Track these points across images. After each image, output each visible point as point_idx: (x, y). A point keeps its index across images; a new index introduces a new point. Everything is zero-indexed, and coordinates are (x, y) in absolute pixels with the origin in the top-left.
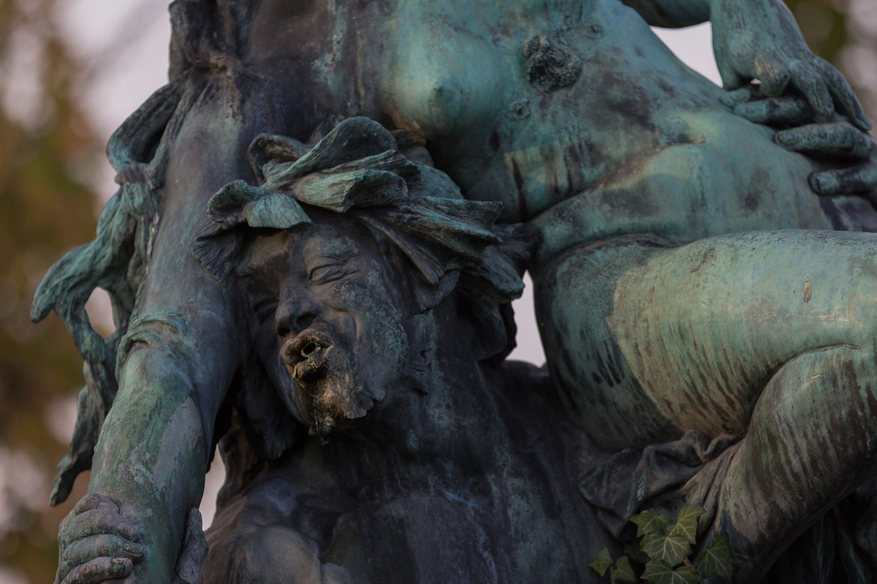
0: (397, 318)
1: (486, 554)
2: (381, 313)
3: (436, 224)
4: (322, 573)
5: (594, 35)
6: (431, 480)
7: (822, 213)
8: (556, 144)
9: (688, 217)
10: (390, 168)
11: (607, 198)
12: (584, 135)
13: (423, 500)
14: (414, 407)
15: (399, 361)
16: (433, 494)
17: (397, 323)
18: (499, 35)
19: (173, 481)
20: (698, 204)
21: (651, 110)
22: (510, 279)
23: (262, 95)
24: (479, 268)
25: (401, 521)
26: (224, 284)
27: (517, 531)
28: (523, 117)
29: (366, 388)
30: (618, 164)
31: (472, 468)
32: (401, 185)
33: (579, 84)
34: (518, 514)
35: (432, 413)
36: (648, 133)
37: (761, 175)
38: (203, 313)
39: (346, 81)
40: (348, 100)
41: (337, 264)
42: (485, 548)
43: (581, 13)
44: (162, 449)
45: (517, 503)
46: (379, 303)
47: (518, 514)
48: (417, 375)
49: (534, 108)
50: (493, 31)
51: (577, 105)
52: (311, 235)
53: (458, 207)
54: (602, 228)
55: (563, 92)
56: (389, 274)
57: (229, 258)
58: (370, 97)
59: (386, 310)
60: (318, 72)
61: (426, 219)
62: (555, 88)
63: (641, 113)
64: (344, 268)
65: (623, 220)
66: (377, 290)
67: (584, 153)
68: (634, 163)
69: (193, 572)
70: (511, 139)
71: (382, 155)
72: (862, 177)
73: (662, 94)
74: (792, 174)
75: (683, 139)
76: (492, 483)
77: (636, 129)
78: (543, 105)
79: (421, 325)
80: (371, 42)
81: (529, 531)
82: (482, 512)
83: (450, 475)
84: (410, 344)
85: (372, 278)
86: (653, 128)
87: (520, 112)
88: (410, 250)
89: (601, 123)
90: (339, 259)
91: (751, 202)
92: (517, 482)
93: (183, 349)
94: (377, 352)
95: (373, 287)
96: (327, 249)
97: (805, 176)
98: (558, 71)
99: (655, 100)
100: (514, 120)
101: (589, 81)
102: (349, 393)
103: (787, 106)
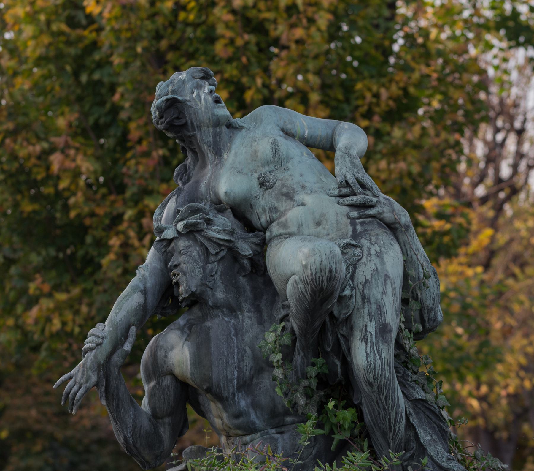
1: (233, 337)
2: (195, 264)
4: (183, 344)
6: (220, 314)
7: (350, 225)
8: (266, 207)
10: (201, 219)
11: (278, 224)
12: (273, 204)
13: (217, 320)
14: (209, 292)
20: (300, 226)
29: (189, 288)
30: (282, 213)
31: (232, 310)
33: (274, 188)
36: (292, 202)
37: (323, 215)
38: (154, 265)
39: (207, 190)
42: (233, 335)
44: (123, 308)
45: (247, 321)
46: (195, 261)
47: (247, 324)
48: (207, 283)
49: (261, 196)
50: (252, 172)
52: (179, 240)
53: (220, 230)
55: (269, 190)
57: (163, 247)
60: (201, 187)
62: (267, 189)
65: (281, 231)
67: (274, 209)
71: (198, 215)
73: (301, 189)
74: (337, 214)
75: (303, 204)
77: (289, 201)
78: (263, 195)
85: (195, 253)
86: (294, 201)
87: (256, 197)
88: (207, 244)
90: (187, 247)
91: (318, 224)
92: (249, 314)
93: (145, 276)
96: (183, 245)
97: (345, 214)
98: (267, 184)
103: (345, 191)
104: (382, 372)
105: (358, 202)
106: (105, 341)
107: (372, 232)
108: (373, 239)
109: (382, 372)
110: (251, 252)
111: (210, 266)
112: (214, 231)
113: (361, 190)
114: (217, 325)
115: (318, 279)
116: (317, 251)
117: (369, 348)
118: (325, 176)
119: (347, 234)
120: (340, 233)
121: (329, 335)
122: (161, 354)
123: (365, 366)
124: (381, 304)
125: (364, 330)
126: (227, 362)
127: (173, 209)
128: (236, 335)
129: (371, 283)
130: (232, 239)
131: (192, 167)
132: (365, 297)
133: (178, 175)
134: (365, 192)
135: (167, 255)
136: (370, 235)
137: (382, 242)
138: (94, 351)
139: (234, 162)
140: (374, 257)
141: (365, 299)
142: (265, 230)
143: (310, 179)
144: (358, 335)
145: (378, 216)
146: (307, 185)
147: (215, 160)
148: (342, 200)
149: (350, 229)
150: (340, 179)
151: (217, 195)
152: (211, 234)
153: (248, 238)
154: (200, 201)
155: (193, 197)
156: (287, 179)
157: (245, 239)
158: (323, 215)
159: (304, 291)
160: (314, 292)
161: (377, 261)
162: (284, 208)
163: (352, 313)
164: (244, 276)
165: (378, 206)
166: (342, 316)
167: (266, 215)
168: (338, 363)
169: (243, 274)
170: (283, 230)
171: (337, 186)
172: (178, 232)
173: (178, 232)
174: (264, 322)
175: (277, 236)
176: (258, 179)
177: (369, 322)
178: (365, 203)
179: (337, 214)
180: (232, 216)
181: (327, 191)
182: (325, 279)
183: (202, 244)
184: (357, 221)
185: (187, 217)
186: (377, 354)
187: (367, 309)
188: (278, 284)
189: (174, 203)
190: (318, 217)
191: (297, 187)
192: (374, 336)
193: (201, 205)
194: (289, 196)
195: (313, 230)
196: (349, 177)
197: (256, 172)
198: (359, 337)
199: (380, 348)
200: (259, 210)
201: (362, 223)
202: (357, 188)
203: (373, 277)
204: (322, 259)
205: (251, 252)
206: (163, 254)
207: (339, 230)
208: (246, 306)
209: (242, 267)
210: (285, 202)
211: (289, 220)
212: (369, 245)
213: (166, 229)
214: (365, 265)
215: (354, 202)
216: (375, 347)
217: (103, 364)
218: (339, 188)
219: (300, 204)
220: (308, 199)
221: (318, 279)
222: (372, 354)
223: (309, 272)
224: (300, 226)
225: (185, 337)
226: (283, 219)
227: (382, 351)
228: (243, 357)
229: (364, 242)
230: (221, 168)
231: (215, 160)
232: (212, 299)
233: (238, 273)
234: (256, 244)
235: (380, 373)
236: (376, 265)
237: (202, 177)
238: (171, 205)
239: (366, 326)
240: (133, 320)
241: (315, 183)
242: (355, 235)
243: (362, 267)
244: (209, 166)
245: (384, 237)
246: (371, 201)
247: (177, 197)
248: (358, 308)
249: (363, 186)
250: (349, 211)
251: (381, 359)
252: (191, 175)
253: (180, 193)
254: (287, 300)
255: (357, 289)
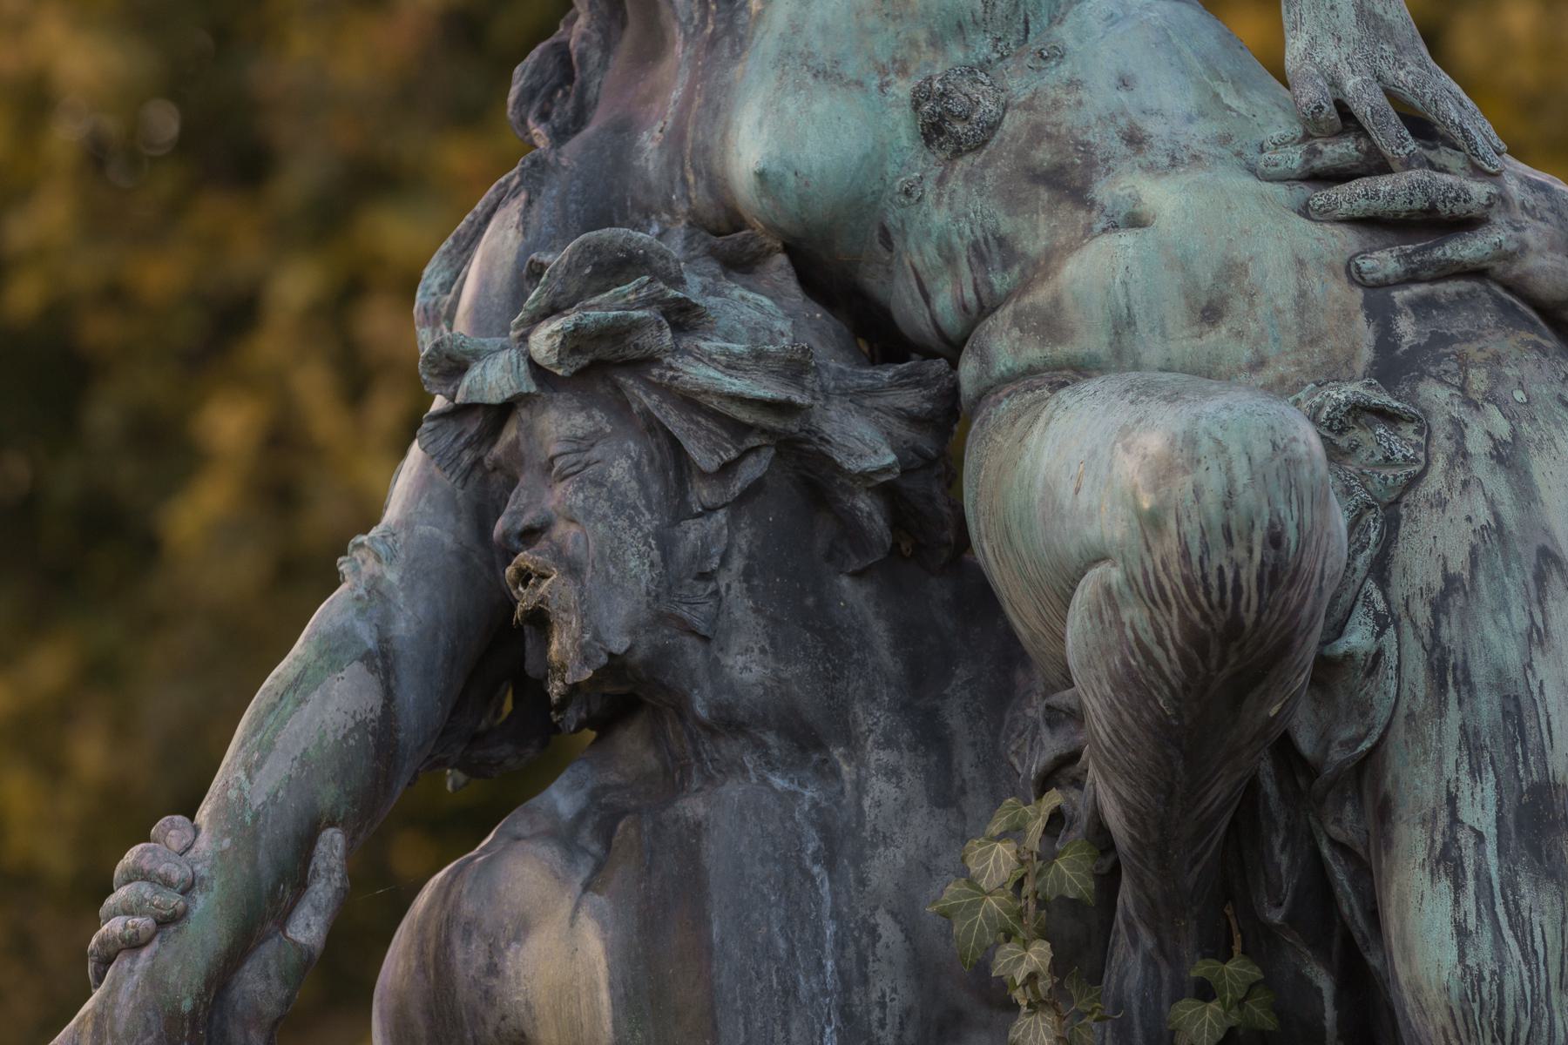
0: (648, 528)
1: (816, 869)
2: (622, 523)
3: (699, 386)
4: (577, 908)
5: (1043, 64)
6: (749, 760)
7: (1361, 318)
8: (955, 239)
9: (1111, 344)
10: (646, 303)
11: (1018, 319)
12: (989, 223)
13: (733, 790)
14: (694, 654)
15: (648, 593)
16: (754, 780)
17: (646, 537)
18: (892, 76)
19: (281, 793)
20: (1123, 324)
21: (1095, 177)
22: (868, 451)
23: (554, 192)
24: (815, 439)
25: (699, 825)
26: (458, 484)
27: (875, 830)
28: (913, 201)
29: (597, 637)
30: (1035, 265)
31: (808, 738)
32: (660, 328)
33: (992, 145)
34: (879, 804)
35: (731, 662)
36: (1082, 215)
37: (1232, 270)
38: (423, 529)
39: (670, 164)
40: (673, 191)
41: (579, 451)
42: (815, 860)
43: (1027, 31)
44: (279, 746)
45: (880, 787)
46: (620, 508)
47: (879, 804)
48: (684, 611)
49: (929, 185)
50: (883, 71)
51: (984, 178)
53: (739, 357)
54: (1009, 364)
55: (969, 158)
56: (652, 461)
57: (468, 445)
58: (702, 184)
59: (631, 518)
60: (641, 150)
61: (687, 378)
62: (958, 153)
63: (1078, 184)
64: (587, 455)
65: (1033, 353)
66: (623, 488)
67: (994, 249)
68: (1054, 263)
69: (308, 925)
70: (904, 233)
71: (632, 286)
72: (1449, 253)
73: (1122, 149)
74: (1301, 263)
75: (1136, 221)
76: (841, 761)
77: (1065, 209)
78: (941, 181)
79: (692, 536)
80: (708, 101)
81: (896, 830)
82: (824, 804)
83: (776, 752)
84: (666, 566)
85: (619, 470)
87: (908, 193)
88: (675, 422)
89: (1013, 202)
90: (582, 443)
91: (1211, 313)
92: (887, 757)
93: (382, 586)
94: (615, 581)
95: (615, 484)
96: (564, 430)
97: (1340, 261)
98: (959, 127)
99: (1106, 160)
100: (903, 206)
101: (1007, 138)
102: (573, 644)
104: (1536, 1019)
105: (1399, 205)
106: (201, 902)
107: (1471, 349)
108: (1479, 380)
109: (1536, 1019)
110: (890, 458)
111: (692, 533)
112: (709, 359)
113: (1412, 145)
114: (738, 812)
115: (1214, 581)
116: (1206, 445)
117: (1469, 903)
118: (1240, 83)
119: (1351, 357)
120: (1318, 355)
121: (1277, 842)
122: (468, 957)
123: (1455, 992)
124: (1521, 691)
125: (1443, 819)
126: (790, 991)
127: (510, 258)
128: (830, 861)
129: (1471, 591)
130: (797, 398)
131: (595, 56)
132: (1443, 661)
133: (529, 95)
134: (1431, 155)
135: (484, 481)
136: (1464, 363)
137: (1519, 395)
138: (145, 954)
139: (796, 28)
140: (1481, 468)
141: (1446, 671)
142: (952, 348)
143: (1168, 100)
144: (1413, 843)
145: (1499, 267)
146: (1152, 127)
147: (704, 20)
148: (1321, 197)
149: (1364, 332)
150: (1311, 93)
151: (717, 185)
152: (698, 374)
153: (872, 391)
154: (636, 217)
155: (606, 199)
156: (1056, 104)
157: (857, 397)
158: (1232, 270)
159: (1148, 638)
160: (1196, 642)
161: (1498, 484)
162: (1043, 243)
163: (1382, 738)
164: (857, 575)
165: (1498, 220)
166: (1337, 755)
167: (956, 275)
168: (1325, 983)
169: (855, 564)
170: (1042, 344)
171: (1298, 131)
172: (538, 371)
173: (538, 371)
174: (963, 791)
175: (1012, 378)
176: (916, 106)
177: (1465, 779)
178: (1433, 209)
179: (1301, 263)
180: (793, 286)
181: (1251, 154)
182: (1249, 576)
183: (653, 426)
184: (1399, 296)
185: (579, 296)
186: (1507, 933)
187: (1453, 717)
188: (1023, 612)
189: (511, 233)
190: (1206, 276)
191: (1107, 140)
192: (1491, 848)
193: (644, 238)
194: (1067, 182)
195: (1185, 343)
196: (1351, 83)
197: (903, 71)
198: (1421, 854)
199: (1524, 903)
200: (921, 253)
201: (1422, 307)
202: (1394, 139)
203: (1483, 564)
204: (1231, 481)
205: (890, 458)
206: (466, 476)
207: (1313, 342)
208: (872, 718)
209: (851, 531)
210: (1050, 213)
211: (1068, 301)
212: (1459, 411)
213: (476, 355)
214: (1442, 504)
215: (1378, 206)
216: (1499, 900)
217: (194, 1012)
218: (1307, 136)
219: (1120, 219)
220: (1162, 197)
221: (1214, 581)
222: (1487, 936)
223: (1171, 544)
224: (1123, 324)
225: (584, 869)
226: (1040, 296)
227: (1536, 918)
228: (862, 961)
229: (1436, 395)
230: (735, 57)
231: (704, 20)
232: (708, 688)
233: (829, 557)
234: (912, 419)
235: (1526, 1023)
236: (1492, 503)
237: (648, 100)
238: (501, 239)
239: (1452, 800)
240: (328, 795)
241: (1190, 119)
242: (1391, 365)
243: (1424, 516)
244: (678, 48)
245: (1529, 369)
246: (1462, 196)
247: (529, 203)
248: (1411, 716)
249: (1421, 126)
250: (1356, 248)
251: (1528, 954)
252: (590, 95)
253: (541, 182)
254: (1070, 684)
255: (1405, 622)
